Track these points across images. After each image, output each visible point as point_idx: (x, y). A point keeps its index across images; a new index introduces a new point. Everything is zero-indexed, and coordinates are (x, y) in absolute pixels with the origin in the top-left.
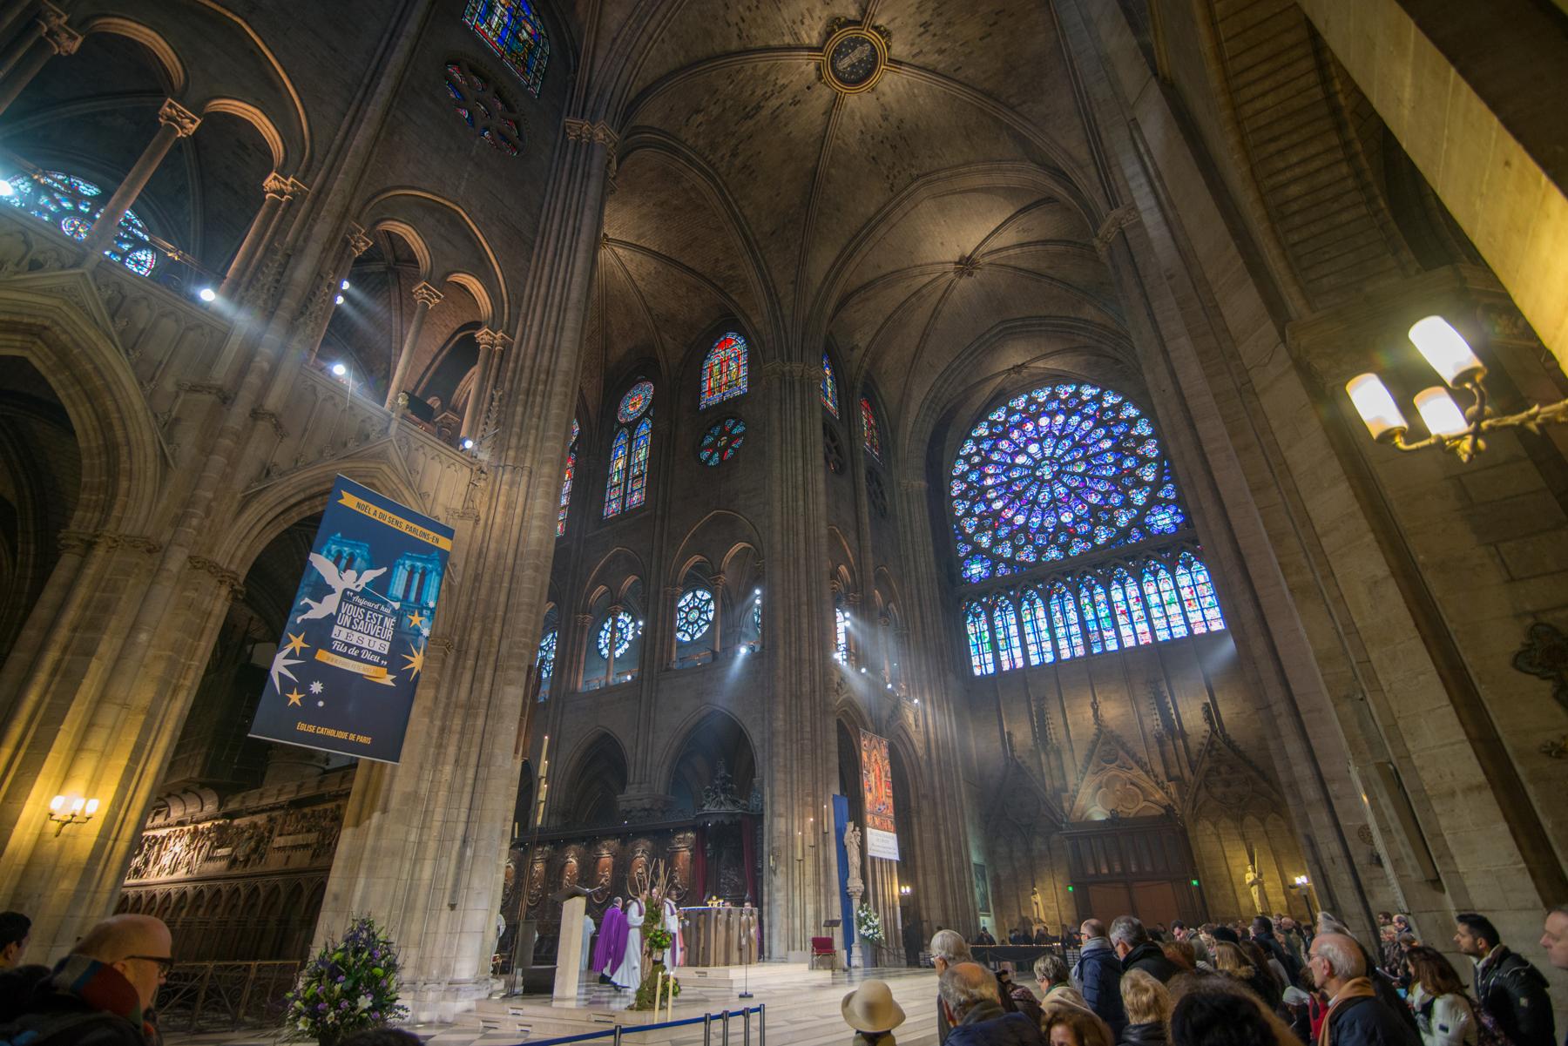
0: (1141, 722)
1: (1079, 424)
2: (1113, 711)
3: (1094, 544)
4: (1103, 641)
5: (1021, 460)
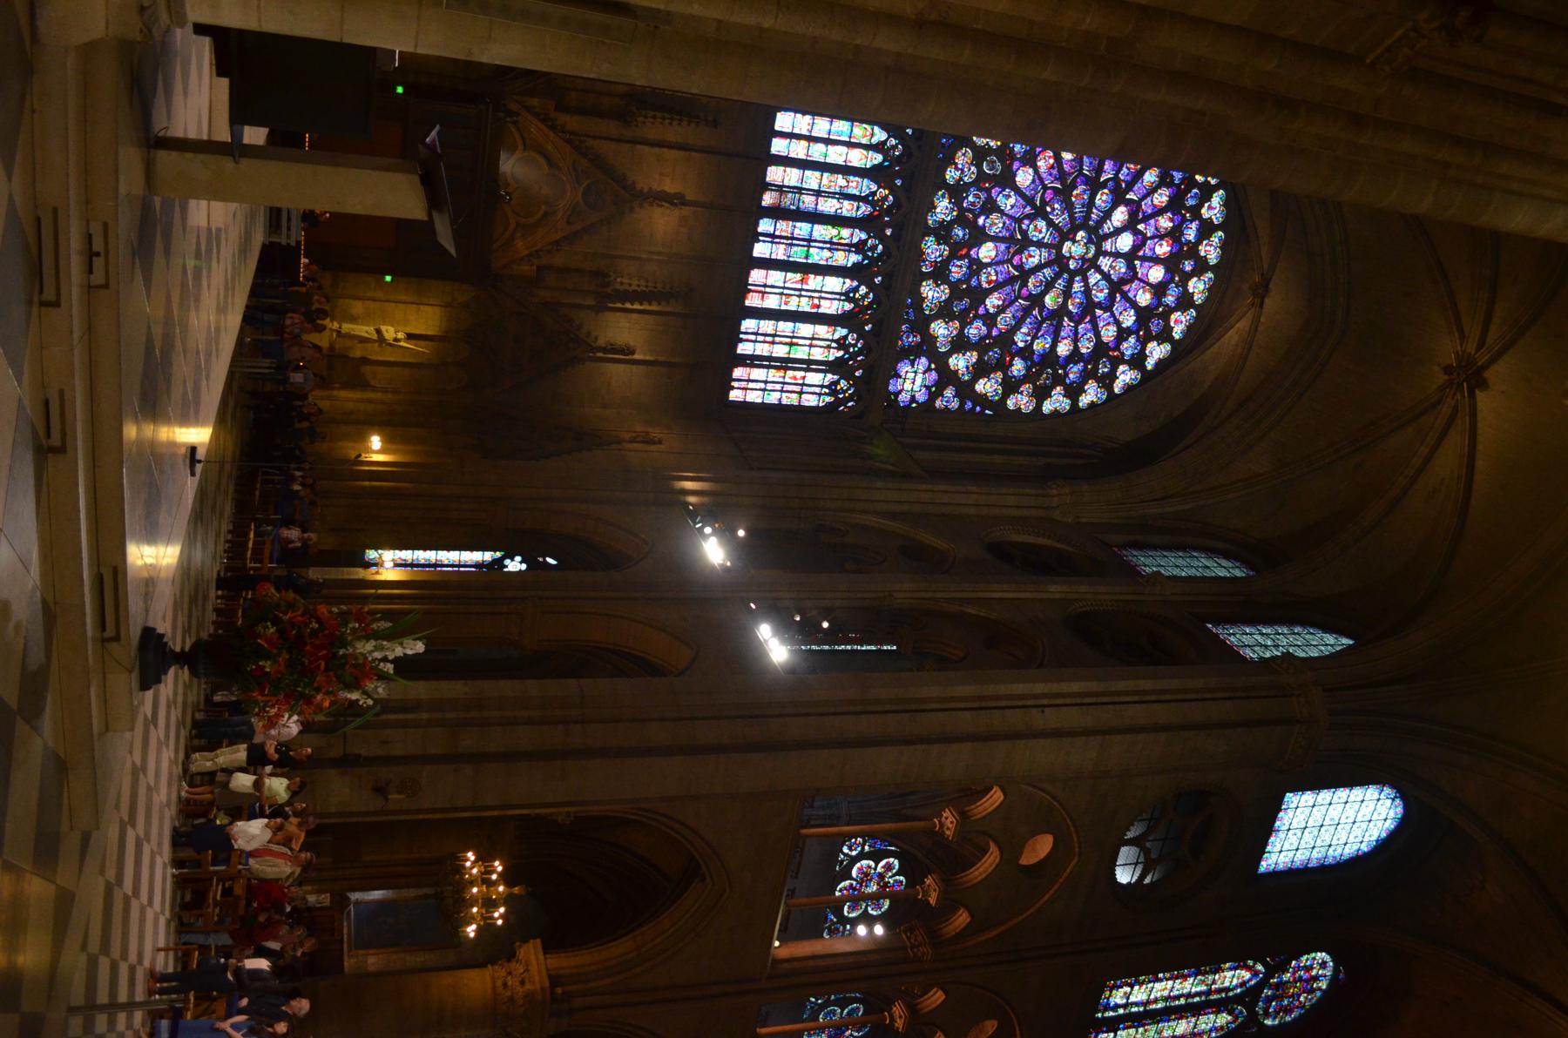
0: (634, 258)
1: (1117, 323)
2: (662, 224)
5: (1120, 216)
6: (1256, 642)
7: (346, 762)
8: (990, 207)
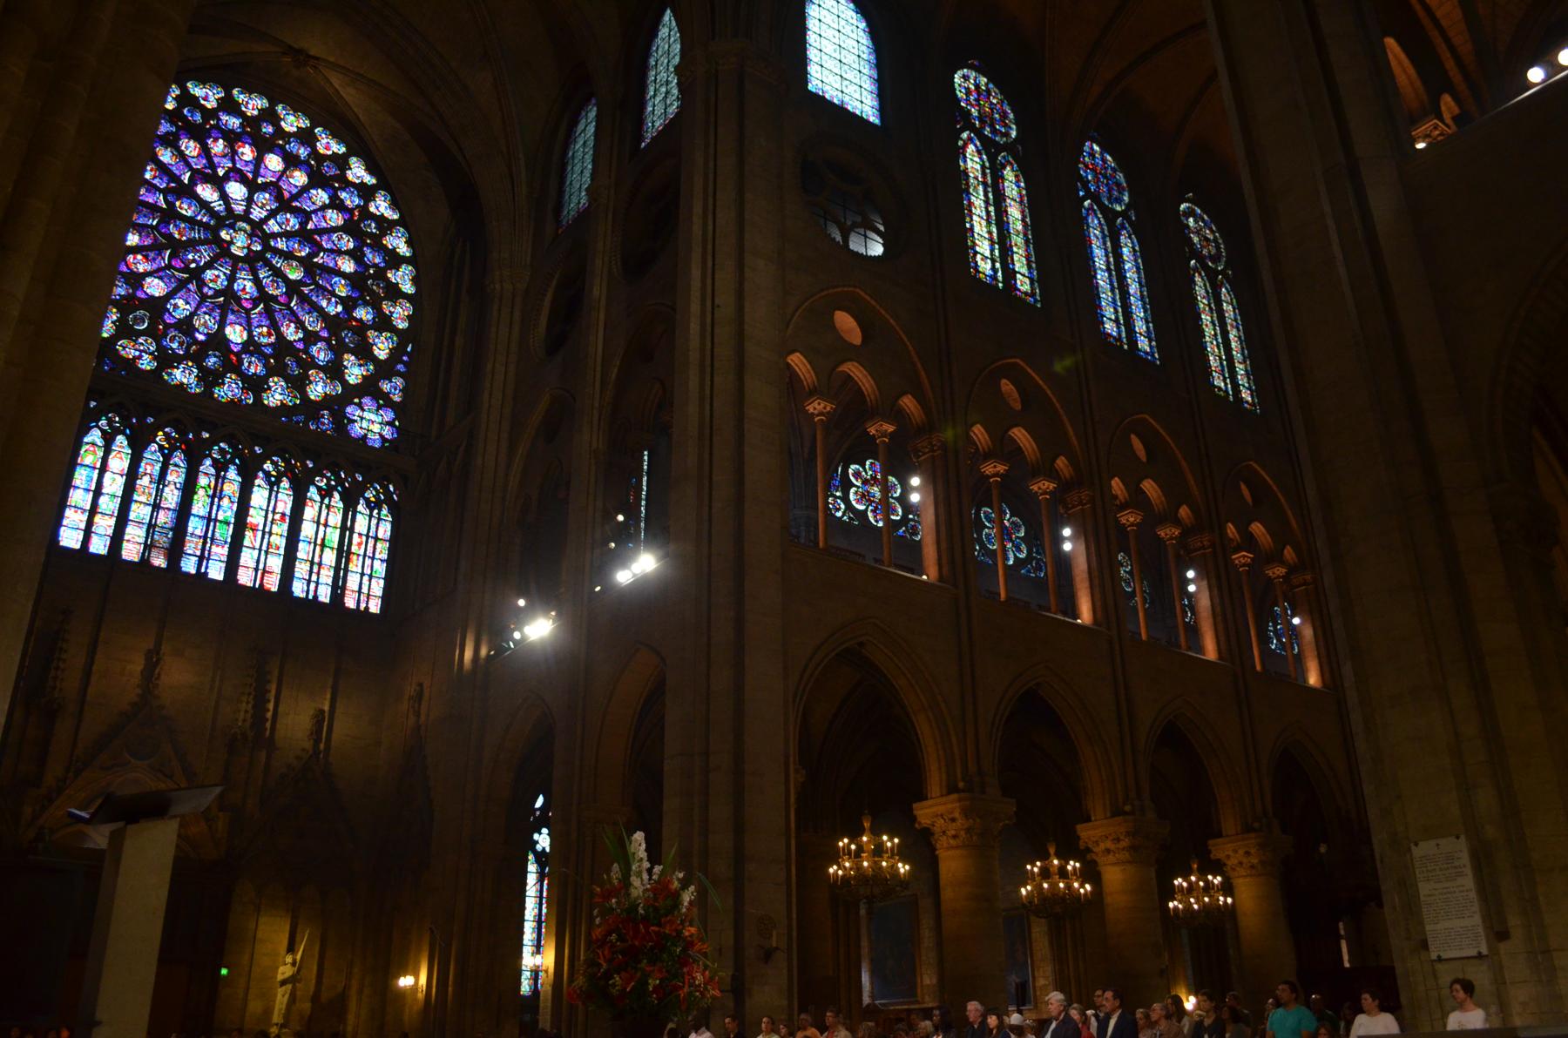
2: (180, 676)
5: (206, 192)
6: (662, 100)
7: (738, 989)
8: (186, 326)
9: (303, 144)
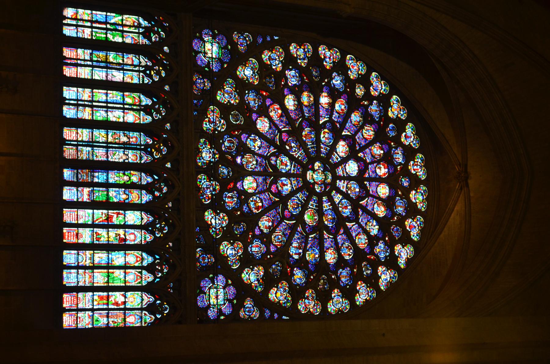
1: (366, 232)
3: (206, 208)
4: (77, 184)
5: (342, 148)
8: (243, 150)
9: (406, 209)
